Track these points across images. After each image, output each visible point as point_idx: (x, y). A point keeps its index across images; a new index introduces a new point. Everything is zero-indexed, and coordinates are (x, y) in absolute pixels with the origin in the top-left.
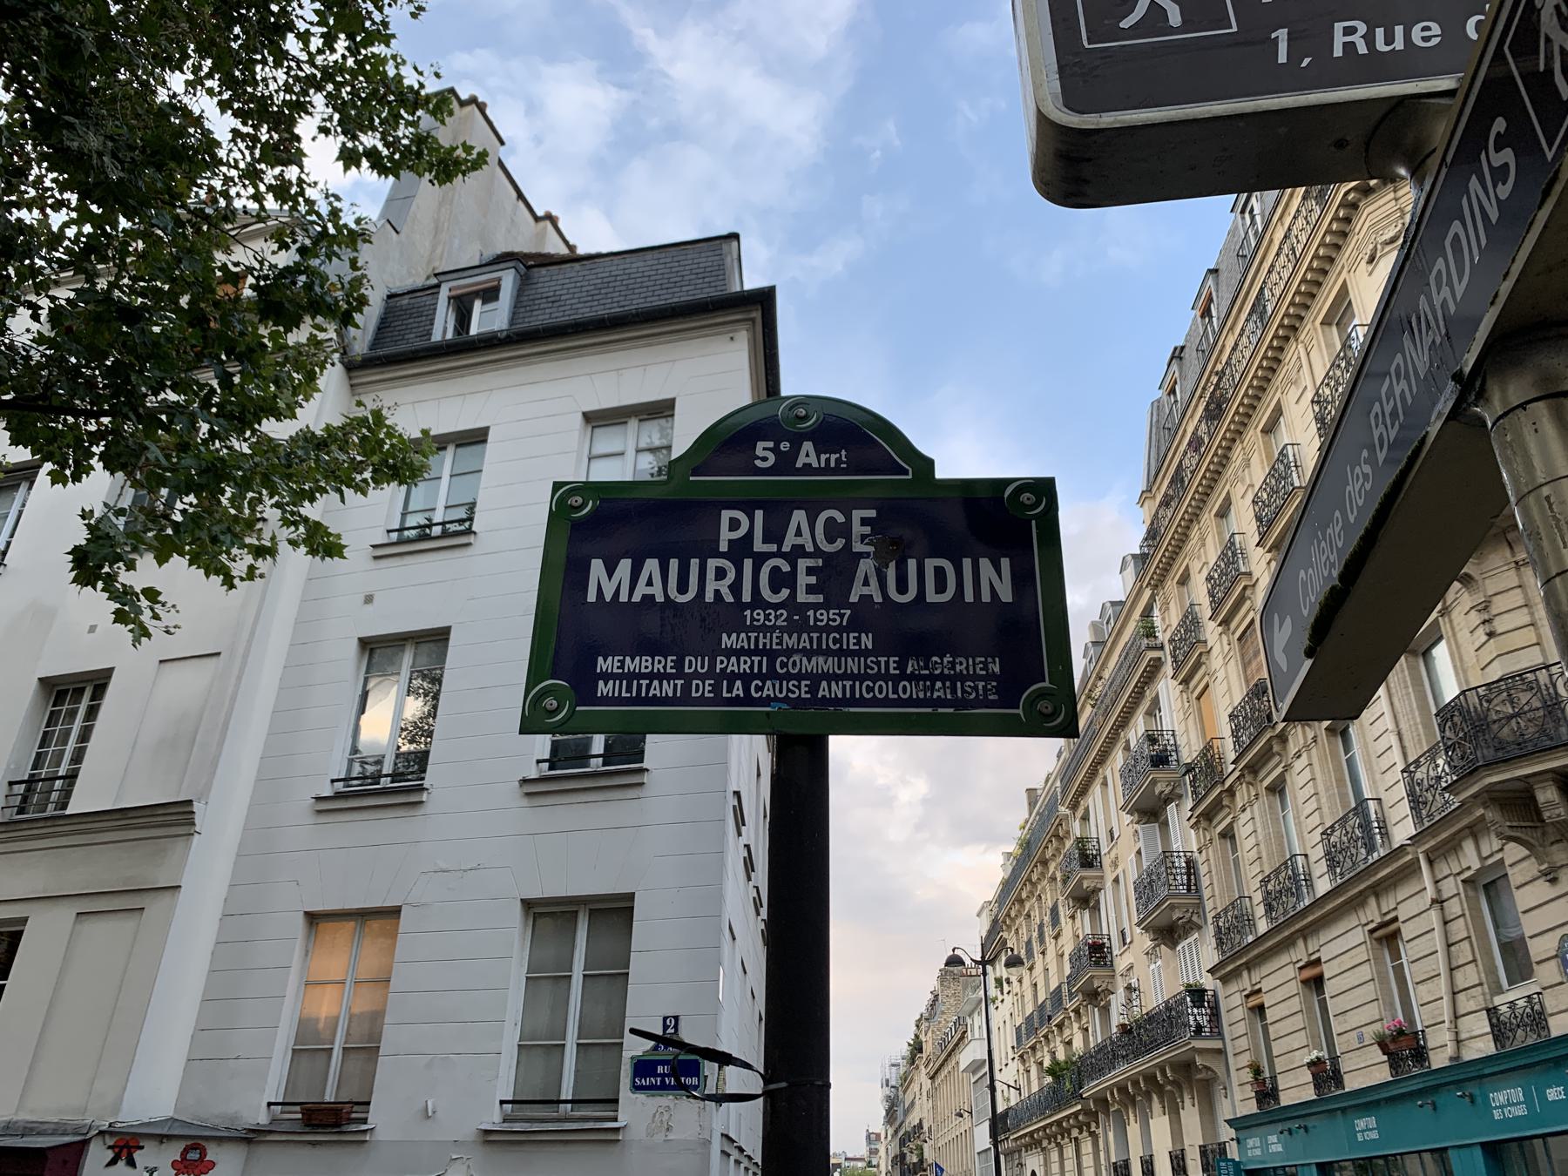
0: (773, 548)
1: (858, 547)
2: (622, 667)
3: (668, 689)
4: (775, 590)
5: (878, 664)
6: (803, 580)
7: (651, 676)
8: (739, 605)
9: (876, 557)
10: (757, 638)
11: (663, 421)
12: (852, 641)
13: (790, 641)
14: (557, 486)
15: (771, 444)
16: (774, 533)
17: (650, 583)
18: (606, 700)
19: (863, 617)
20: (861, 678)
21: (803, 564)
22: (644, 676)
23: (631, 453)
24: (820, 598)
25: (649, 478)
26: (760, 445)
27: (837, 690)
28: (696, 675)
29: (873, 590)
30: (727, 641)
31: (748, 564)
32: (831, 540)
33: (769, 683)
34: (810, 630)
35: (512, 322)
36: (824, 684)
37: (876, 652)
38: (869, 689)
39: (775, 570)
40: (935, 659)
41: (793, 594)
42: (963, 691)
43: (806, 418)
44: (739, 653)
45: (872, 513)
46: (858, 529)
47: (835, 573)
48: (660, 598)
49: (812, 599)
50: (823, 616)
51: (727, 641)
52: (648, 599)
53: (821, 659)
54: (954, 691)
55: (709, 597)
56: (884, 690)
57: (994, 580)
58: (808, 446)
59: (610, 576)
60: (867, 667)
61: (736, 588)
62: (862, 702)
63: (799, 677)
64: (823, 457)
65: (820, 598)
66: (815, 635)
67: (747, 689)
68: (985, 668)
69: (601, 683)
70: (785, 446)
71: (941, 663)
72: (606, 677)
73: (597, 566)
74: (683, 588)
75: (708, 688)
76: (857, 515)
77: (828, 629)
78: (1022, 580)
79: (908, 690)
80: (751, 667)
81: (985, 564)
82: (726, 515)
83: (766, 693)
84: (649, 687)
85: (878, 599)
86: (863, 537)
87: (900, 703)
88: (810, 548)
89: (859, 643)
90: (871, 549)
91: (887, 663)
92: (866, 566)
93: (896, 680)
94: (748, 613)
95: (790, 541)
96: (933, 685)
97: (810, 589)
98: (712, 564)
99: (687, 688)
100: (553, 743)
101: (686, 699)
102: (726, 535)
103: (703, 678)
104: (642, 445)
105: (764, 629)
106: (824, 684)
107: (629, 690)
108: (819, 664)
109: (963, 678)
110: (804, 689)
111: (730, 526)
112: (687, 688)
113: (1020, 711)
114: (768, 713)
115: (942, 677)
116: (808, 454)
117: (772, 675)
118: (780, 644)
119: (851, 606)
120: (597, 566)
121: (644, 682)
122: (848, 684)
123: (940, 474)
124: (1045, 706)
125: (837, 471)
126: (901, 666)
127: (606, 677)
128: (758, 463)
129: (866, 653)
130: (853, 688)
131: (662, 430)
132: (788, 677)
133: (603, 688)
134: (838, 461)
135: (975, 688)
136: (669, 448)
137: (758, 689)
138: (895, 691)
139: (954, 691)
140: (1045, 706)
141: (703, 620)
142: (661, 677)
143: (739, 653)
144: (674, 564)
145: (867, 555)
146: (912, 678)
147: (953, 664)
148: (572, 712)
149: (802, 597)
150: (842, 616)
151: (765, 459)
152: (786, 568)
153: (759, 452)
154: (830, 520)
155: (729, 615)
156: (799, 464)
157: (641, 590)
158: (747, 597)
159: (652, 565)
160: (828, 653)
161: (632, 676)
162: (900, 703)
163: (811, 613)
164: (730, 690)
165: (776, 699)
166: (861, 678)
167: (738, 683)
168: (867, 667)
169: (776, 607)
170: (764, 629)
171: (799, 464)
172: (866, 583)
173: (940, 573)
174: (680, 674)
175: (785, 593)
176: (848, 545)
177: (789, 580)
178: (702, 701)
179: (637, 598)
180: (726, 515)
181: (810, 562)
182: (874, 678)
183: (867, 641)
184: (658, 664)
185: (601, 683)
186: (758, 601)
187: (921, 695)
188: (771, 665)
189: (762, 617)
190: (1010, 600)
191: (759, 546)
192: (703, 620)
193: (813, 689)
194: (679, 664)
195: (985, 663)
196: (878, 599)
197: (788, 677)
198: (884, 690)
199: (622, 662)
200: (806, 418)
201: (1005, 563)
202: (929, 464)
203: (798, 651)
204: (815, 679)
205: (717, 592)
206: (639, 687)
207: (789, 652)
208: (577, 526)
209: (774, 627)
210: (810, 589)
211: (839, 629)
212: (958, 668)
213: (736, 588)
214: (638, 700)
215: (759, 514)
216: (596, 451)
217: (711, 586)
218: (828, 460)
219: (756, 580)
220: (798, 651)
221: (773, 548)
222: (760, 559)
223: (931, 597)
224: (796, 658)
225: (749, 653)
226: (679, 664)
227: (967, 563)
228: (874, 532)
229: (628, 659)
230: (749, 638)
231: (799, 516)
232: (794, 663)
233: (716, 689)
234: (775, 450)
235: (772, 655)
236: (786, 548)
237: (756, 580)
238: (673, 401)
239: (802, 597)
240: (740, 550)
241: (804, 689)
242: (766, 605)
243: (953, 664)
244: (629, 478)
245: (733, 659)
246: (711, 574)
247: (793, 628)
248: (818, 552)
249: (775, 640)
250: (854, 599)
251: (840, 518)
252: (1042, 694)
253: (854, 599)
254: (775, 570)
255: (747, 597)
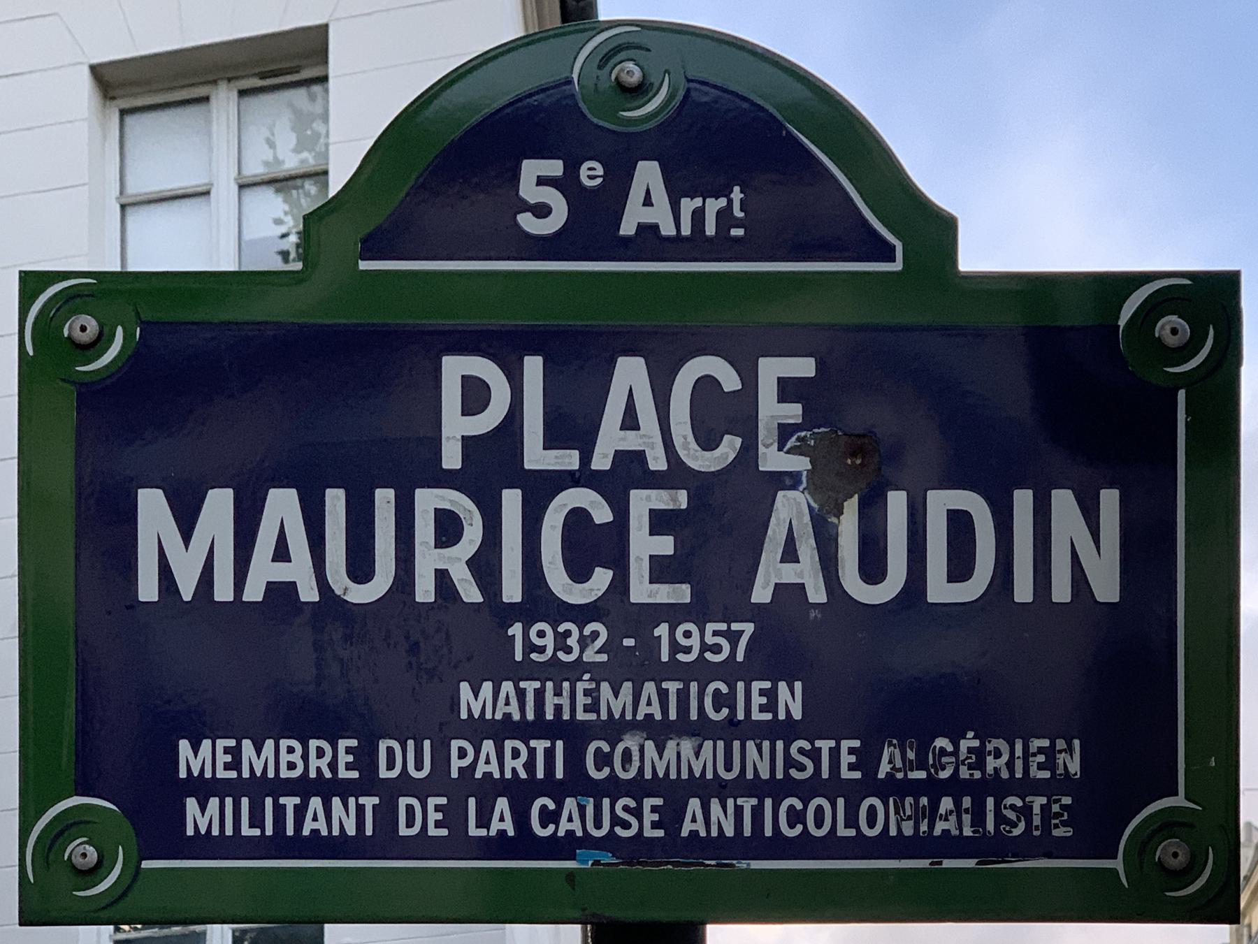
0: (570, 460)
1: (773, 459)
2: (235, 765)
3: (345, 817)
4: (579, 573)
5: (815, 755)
6: (645, 546)
7: (305, 787)
8: (506, 614)
9: (813, 489)
10: (539, 694)
11: (299, 96)
12: (757, 700)
13: (616, 702)
14: (31, 283)
15: (555, 168)
16: (572, 425)
17: (281, 553)
18: (205, 845)
19: (784, 641)
20: (776, 789)
21: (642, 502)
22: (289, 787)
23: (225, 190)
24: (682, 593)
25: (277, 265)
26: (531, 169)
27: (722, 819)
28: (404, 784)
29: (806, 573)
30: (474, 701)
31: (512, 500)
32: (708, 441)
33: (570, 804)
34: (661, 673)
35: (559, 158)
36: (694, 804)
37: (806, 729)
38: (796, 817)
39: (578, 518)
40: (942, 743)
41: (620, 584)
42: (1000, 819)
43: (640, 91)
44: (503, 730)
45: (804, 367)
46: (773, 411)
47: (717, 526)
48: (309, 593)
49: (666, 594)
50: (691, 637)
51: (474, 701)
52: (281, 593)
53: (687, 746)
54: (979, 820)
55: (425, 591)
56: (829, 816)
57: (1080, 544)
58: (648, 174)
59: (187, 536)
60: (789, 763)
61: (485, 565)
62: (779, 847)
63: (639, 788)
64: (688, 205)
65: (682, 593)
66: (672, 687)
67: (521, 818)
68: (1050, 764)
69: (191, 804)
70: (591, 173)
71: (954, 752)
72: (204, 788)
73: (152, 506)
74: (361, 569)
75: (434, 816)
76: (771, 370)
77: (701, 671)
78: (1145, 549)
79: (883, 817)
80: (530, 766)
81: (1063, 501)
82: (455, 368)
83: (564, 827)
84: (300, 812)
85: (817, 594)
86: (785, 432)
87: (861, 847)
88: (657, 462)
89: (771, 706)
90: (801, 464)
91: (835, 753)
92: (791, 509)
93: (854, 793)
94: (516, 630)
95: (610, 441)
96: (935, 805)
97: (661, 570)
98: (428, 501)
99: (386, 814)
100: (234, 931)
101: (385, 841)
102: (456, 428)
103: (422, 790)
104: (255, 168)
105: (557, 671)
106: (694, 804)
107: (257, 821)
108: (687, 757)
109: (998, 787)
110: (649, 817)
111: (471, 399)
112: (386, 814)
113: (1118, 864)
114: (570, 875)
115: (955, 787)
116: (649, 201)
117: (577, 783)
118: (593, 707)
119: (757, 613)
120: (152, 506)
121: (290, 802)
122: (748, 804)
123: (975, 256)
124: (1171, 852)
125: (721, 247)
126: (866, 760)
127: (204, 788)
128: (527, 222)
129: (785, 730)
130: (757, 813)
131: (301, 122)
132: (614, 788)
133: (198, 817)
134: (724, 216)
135: (1026, 811)
136: (321, 175)
137: (549, 817)
138: (851, 821)
139: (979, 820)
140: (1171, 852)
141: (414, 649)
142: (328, 788)
143: (503, 730)
144: (335, 501)
145: (787, 480)
146: (893, 789)
147: (980, 755)
148: (134, 874)
149: (642, 591)
150: (733, 638)
151: (542, 211)
152: (602, 514)
153: (529, 191)
154: (706, 385)
155: (466, 635)
156: (627, 228)
157: (263, 571)
158: (512, 591)
159: (282, 505)
160: (701, 730)
161: (262, 787)
162: (861, 847)
163: (662, 630)
164: (484, 822)
165: (588, 841)
166: (776, 789)
167: (502, 804)
168: (789, 763)
169: (582, 614)
170: (557, 671)
171: (627, 228)
172: (790, 554)
173: (960, 523)
174: (368, 782)
175: (602, 578)
176: (749, 451)
177: (592, 546)
178: (422, 846)
179: (254, 592)
180: (455, 368)
181: (660, 499)
182: (806, 791)
183: (791, 701)
184: (330, 757)
185: (191, 804)
186: (540, 601)
187: (908, 829)
188: (575, 759)
189: (549, 641)
190: (1115, 598)
191: (537, 456)
192: (414, 649)
193: (671, 817)
194: (365, 758)
195: (1050, 753)
196: (817, 594)
197: (614, 788)
198: (829, 816)
199: (236, 752)
200: (640, 91)
201: (1110, 499)
202: (937, 230)
203: (634, 726)
204: (675, 793)
205: (442, 577)
206: (279, 811)
207: (614, 729)
208: (95, 398)
209: (579, 667)
210: (661, 570)
211: (729, 671)
212: (991, 763)
213: (485, 565)
214: (280, 845)
215: (533, 367)
216: (140, 185)
217: (428, 560)
218: (698, 215)
219: (533, 546)
220: (634, 726)
221: (570, 460)
222: (538, 490)
223: (940, 590)
224: (630, 742)
225: (525, 731)
226: (365, 758)
227: (1023, 500)
228: (809, 421)
229: (247, 746)
230: (521, 694)
231: (630, 374)
232: (627, 755)
233: (453, 817)
234: (567, 184)
235: (574, 734)
236: (601, 461)
237: (533, 546)
238: (322, 32)
239: (642, 591)
240: (492, 464)
241: (649, 817)
242: (560, 611)
243: (980, 753)
244: (227, 263)
245: (488, 746)
246: (424, 529)
247: (634, 665)
248: (677, 474)
249: (581, 700)
250: (761, 594)
251: (730, 380)
252: (1168, 824)
253: (761, 594)
254: (578, 518)
255: (512, 591)
